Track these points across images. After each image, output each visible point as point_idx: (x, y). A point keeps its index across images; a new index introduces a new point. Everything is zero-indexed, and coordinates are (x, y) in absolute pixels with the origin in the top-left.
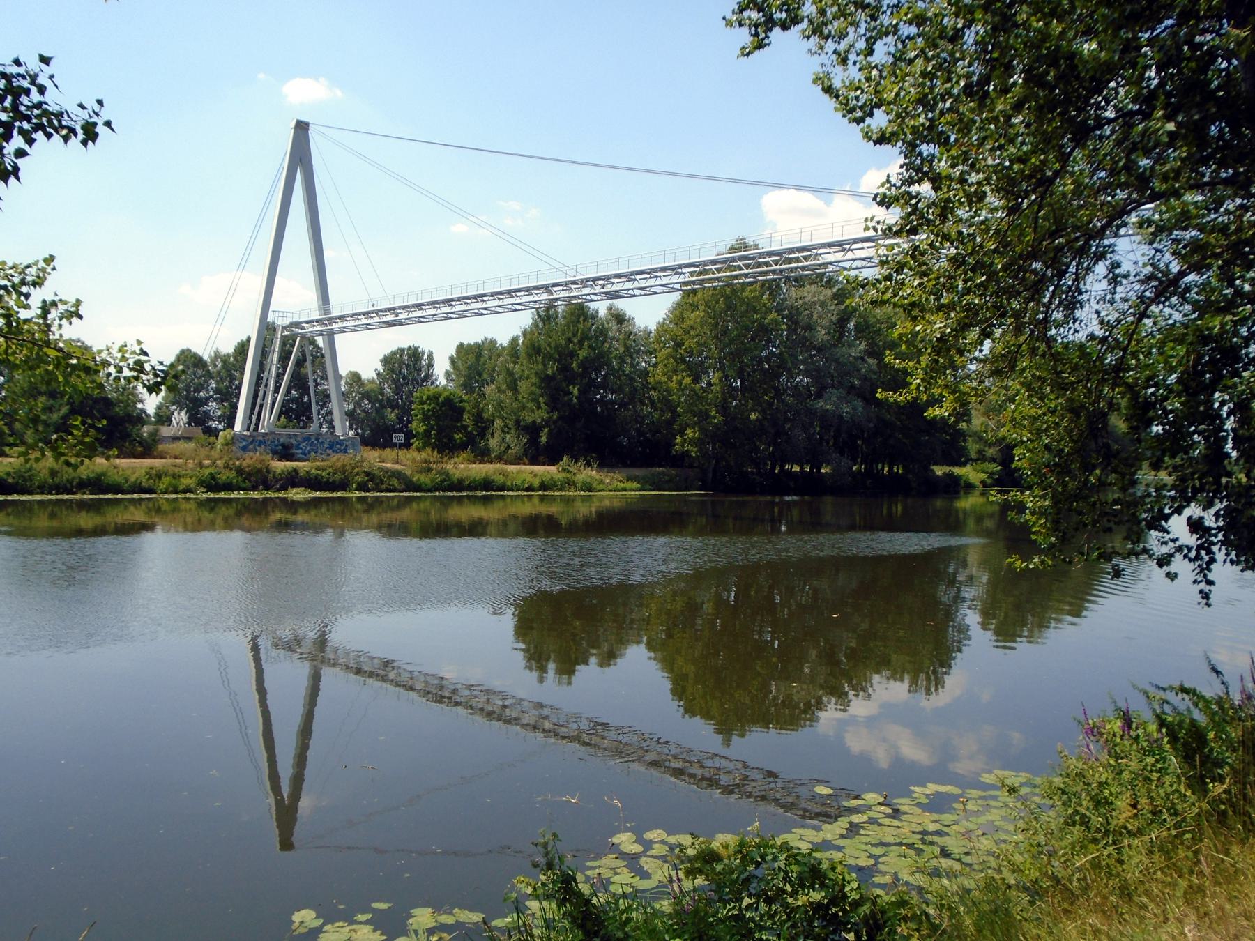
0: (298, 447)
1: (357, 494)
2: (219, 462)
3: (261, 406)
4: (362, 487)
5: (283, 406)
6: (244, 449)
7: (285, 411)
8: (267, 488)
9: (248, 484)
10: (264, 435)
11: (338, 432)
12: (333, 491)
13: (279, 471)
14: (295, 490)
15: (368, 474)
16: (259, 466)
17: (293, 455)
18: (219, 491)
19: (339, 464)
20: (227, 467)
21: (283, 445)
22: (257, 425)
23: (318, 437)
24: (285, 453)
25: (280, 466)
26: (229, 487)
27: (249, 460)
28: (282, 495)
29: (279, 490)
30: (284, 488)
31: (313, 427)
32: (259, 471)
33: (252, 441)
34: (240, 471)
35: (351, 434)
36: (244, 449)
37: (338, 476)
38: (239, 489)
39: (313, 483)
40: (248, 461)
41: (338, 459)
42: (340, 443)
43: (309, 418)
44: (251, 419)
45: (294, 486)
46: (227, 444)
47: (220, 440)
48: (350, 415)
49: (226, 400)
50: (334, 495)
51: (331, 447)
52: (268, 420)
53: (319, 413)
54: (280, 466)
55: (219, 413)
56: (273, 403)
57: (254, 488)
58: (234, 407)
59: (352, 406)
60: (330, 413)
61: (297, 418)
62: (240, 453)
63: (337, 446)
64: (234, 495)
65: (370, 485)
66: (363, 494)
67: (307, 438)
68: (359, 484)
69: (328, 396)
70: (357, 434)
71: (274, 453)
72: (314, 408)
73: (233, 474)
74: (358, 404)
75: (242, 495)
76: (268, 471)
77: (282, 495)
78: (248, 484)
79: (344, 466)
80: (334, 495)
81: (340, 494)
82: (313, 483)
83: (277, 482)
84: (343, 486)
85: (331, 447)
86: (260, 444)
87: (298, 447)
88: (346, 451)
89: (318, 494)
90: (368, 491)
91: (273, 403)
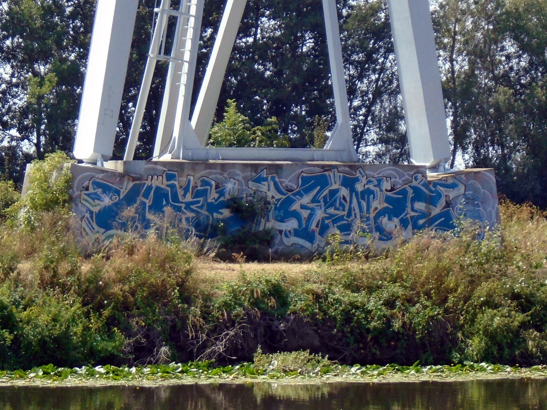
0: (285, 211)
1: (489, 373)
2: (24, 266)
3: (161, 71)
4: (503, 349)
5: (230, 71)
6: (106, 220)
7: (239, 88)
8: (185, 354)
9: (120, 341)
10: (172, 170)
11: (421, 155)
12: (405, 362)
13: (222, 295)
14: (277, 360)
15: (523, 301)
16: (156, 277)
17: (267, 238)
18: (26, 365)
19: (424, 268)
20: (51, 282)
21: (234, 205)
22: (147, 138)
23: (352, 171)
24: (241, 232)
25: (225, 277)
26: (57, 352)
27: (125, 258)
28: (234, 377)
29: (222, 362)
30: (239, 354)
31: (334, 142)
32: (157, 294)
33: (132, 194)
34: (93, 295)
35: (462, 161)
36: (106, 220)
37: (422, 313)
38: (95, 358)
39: (339, 336)
40: (120, 261)
41: (420, 252)
42: (428, 193)
43: (321, 109)
44: (125, 121)
45: (274, 344)
46: (50, 205)
47: (29, 191)
48: (459, 94)
49: (44, 56)
50: (412, 376)
51: (396, 206)
52: (183, 123)
53: (352, 92)
54: (225, 277)
55: (20, 101)
56: (201, 61)
57: (142, 355)
58: (73, 77)
59: (462, 64)
60: (389, 88)
61: (280, 109)
62: (92, 235)
63: (417, 203)
64: (75, 379)
65: (532, 341)
66: (508, 373)
67: (316, 180)
68: (491, 336)
69: (383, 32)
70: (481, 161)
71: (206, 231)
72: (338, 76)
73: (70, 307)
74: (481, 55)
75: (100, 378)
76: (187, 298)
77: (234, 377)
78: (120, 341)
79: (440, 274)
80: (412, 376)
81: (427, 374)
82: (339, 336)
83: (217, 330)
84: (438, 347)
85: (396, 206)
86: (160, 200)
87: (285, 211)
88: (446, 223)
89: (353, 375)
90: (527, 361)
91: (201, 61)
